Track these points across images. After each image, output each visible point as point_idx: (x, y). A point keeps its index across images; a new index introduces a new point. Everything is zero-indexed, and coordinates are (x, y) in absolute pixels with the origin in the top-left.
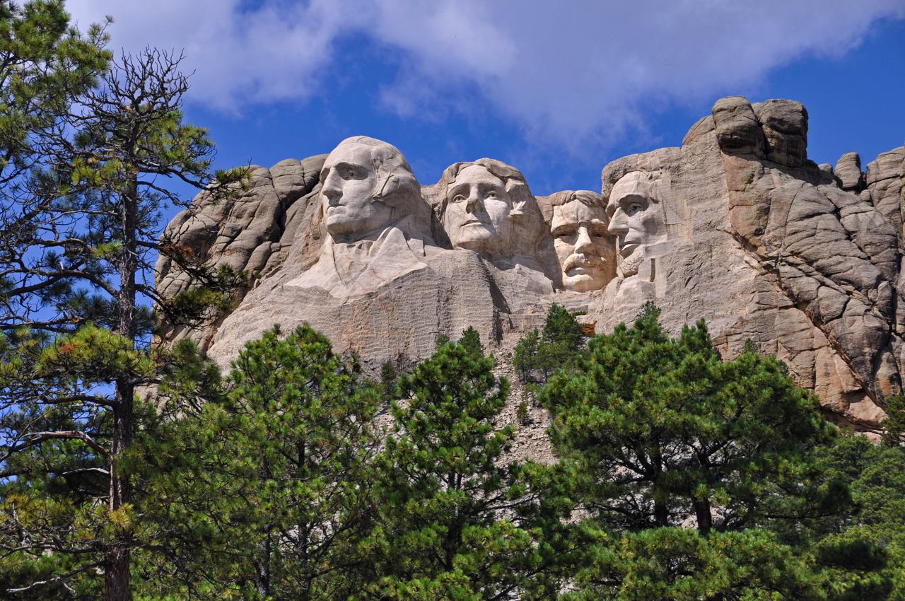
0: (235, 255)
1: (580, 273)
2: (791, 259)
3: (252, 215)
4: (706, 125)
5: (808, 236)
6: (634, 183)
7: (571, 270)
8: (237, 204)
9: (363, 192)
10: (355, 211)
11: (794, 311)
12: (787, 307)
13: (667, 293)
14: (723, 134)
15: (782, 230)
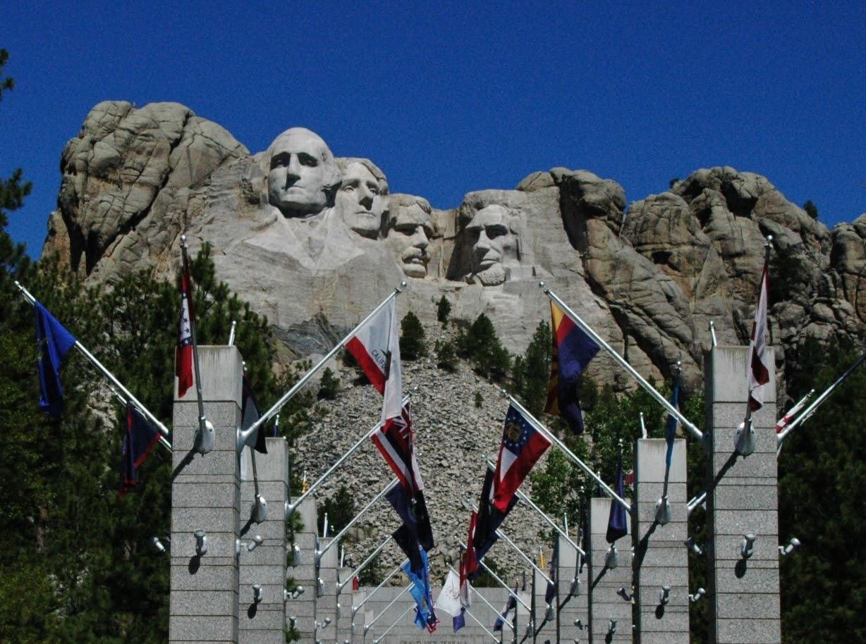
0: (145, 188)
1: (415, 263)
2: (637, 309)
3: (150, 153)
4: (544, 180)
5: (650, 295)
6: (500, 215)
7: (408, 260)
8: (137, 142)
9: (318, 180)
10: (310, 195)
11: (637, 348)
12: (634, 345)
13: (539, 312)
14: (593, 203)
15: (628, 285)
